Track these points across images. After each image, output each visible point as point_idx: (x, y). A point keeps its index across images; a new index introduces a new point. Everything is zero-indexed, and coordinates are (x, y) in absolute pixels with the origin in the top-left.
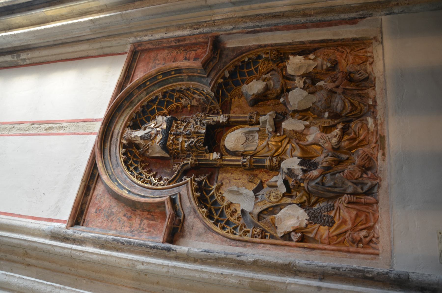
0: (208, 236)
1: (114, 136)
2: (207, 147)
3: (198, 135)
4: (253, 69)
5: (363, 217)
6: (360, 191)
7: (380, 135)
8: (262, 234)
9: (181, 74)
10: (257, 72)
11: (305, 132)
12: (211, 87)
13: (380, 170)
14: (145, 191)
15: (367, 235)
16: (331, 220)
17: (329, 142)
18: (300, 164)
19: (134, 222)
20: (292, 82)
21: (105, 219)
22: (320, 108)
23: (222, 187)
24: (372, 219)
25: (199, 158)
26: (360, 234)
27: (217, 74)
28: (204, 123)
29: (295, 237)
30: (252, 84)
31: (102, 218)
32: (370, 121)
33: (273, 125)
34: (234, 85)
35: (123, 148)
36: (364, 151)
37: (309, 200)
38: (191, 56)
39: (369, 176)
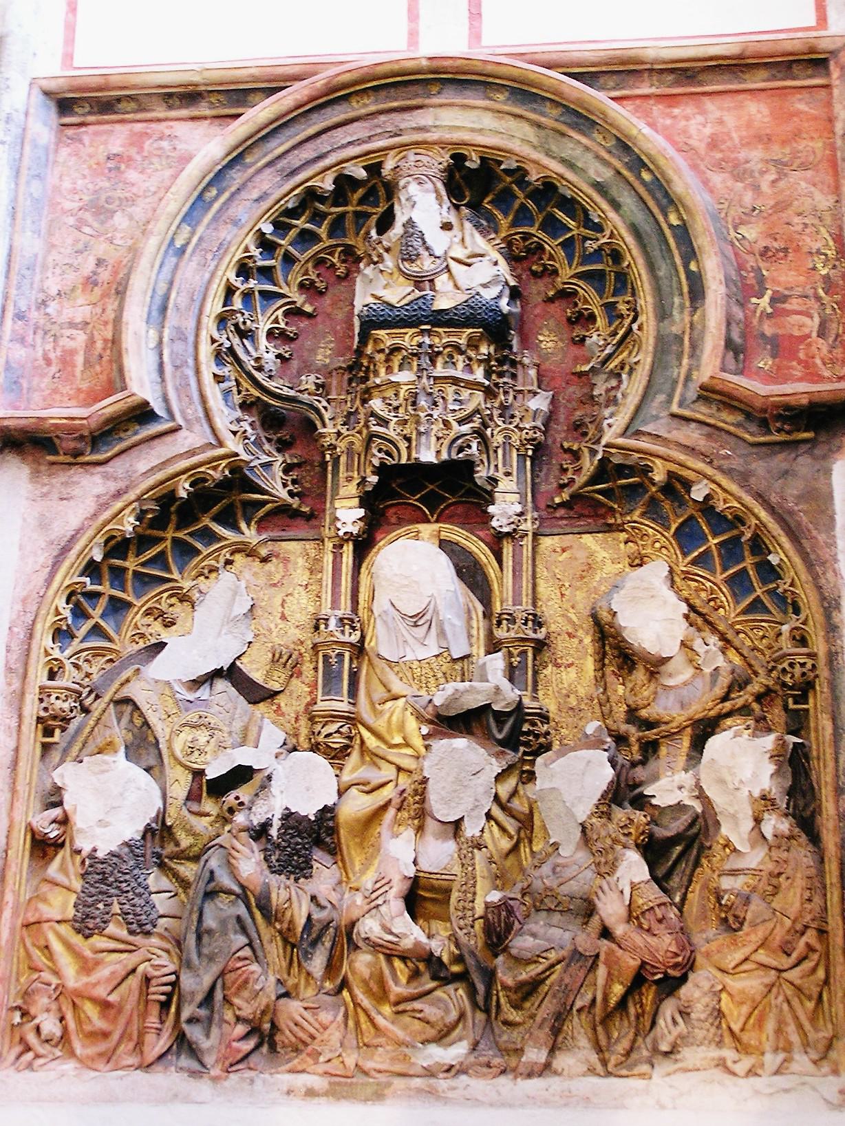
0: (40, 552)
1: (406, 116)
2: (374, 479)
3: (414, 436)
4: (759, 592)
5: (99, 1023)
6: (185, 1015)
7: (389, 1085)
8: (54, 718)
9: (688, 304)
10: (744, 612)
11: (431, 825)
12: (620, 441)
13: (252, 1081)
14: (188, 308)
15: (43, 1037)
16: (91, 926)
17: (367, 908)
18: (288, 816)
19: (80, 301)
20: (682, 760)
21: (86, 198)
22: (536, 873)
23: (257, 563)
24: (91, 1051)
25: (343, 459)
26: (45, 1015)
27: (691, 450)
28: (469, 447)
29: (44, 821)
30: (665, 602)
31: (90, 186)
32: (456, 1052)
33: (466, 708)
34: (677, 529)
35: (365, 168)
36: (325, 1028)
37: (182, 856)
38: (795, 318)
39: (235, 1044)
